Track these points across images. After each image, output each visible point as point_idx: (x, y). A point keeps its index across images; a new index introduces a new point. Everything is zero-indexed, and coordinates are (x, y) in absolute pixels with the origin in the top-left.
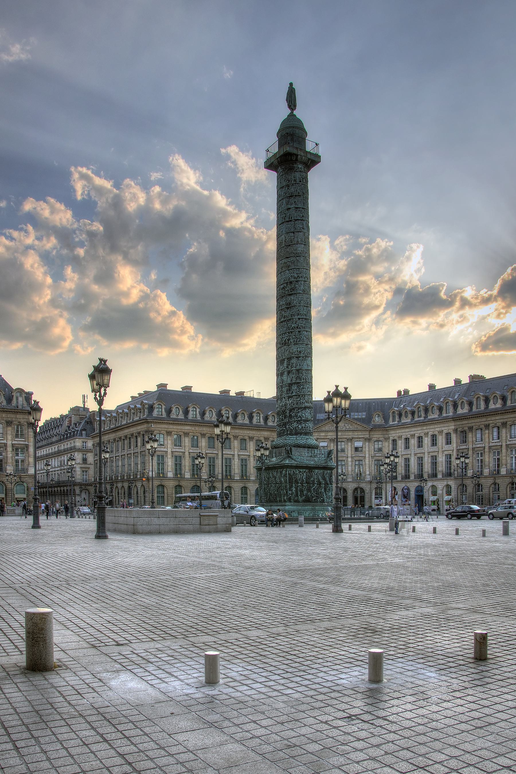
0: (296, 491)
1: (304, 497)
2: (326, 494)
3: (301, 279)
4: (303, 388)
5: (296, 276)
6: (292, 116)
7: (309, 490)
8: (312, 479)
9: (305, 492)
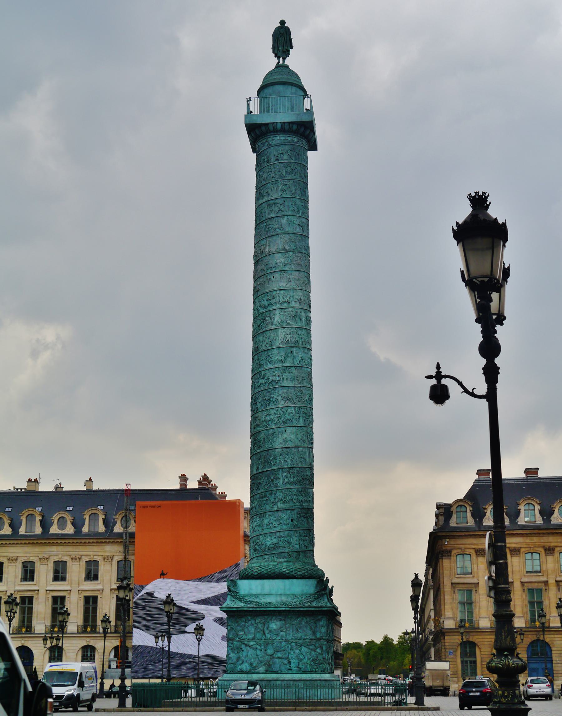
3: (274, 307)
5: (266, 303)
6: (281, 68)
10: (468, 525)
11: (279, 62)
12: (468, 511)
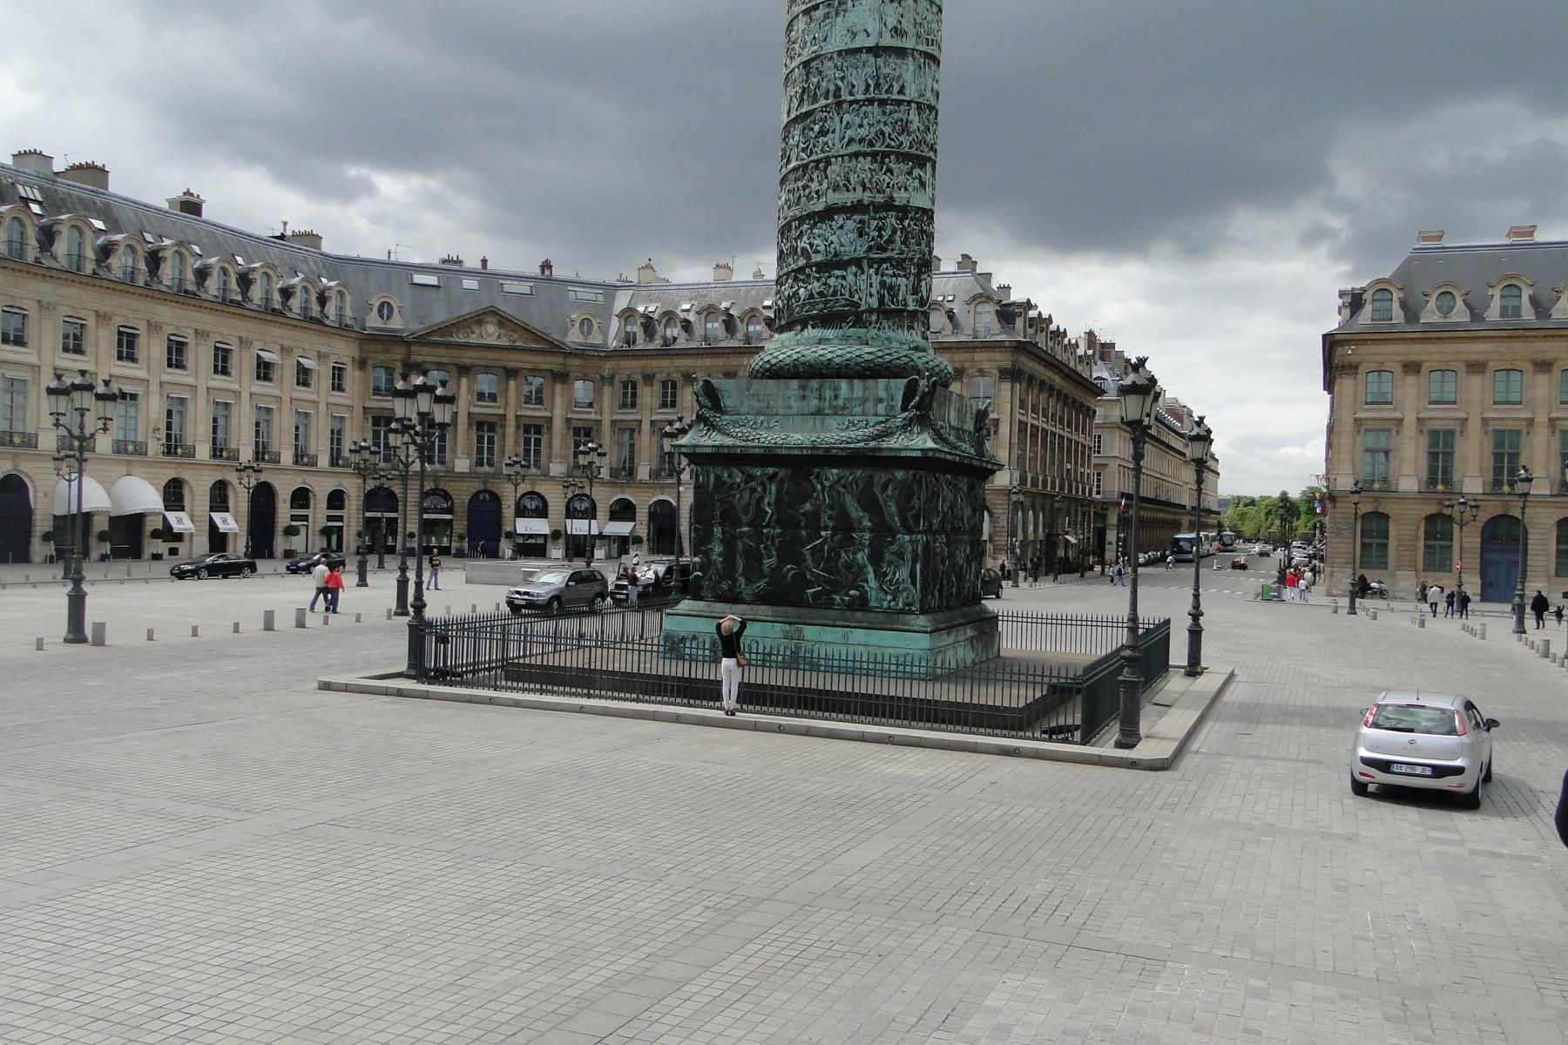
0: (729, 555)
1: (762, 583)
2: (880, 575)
4: (823, 132)
7: (790, 553)
8: (808, 507)
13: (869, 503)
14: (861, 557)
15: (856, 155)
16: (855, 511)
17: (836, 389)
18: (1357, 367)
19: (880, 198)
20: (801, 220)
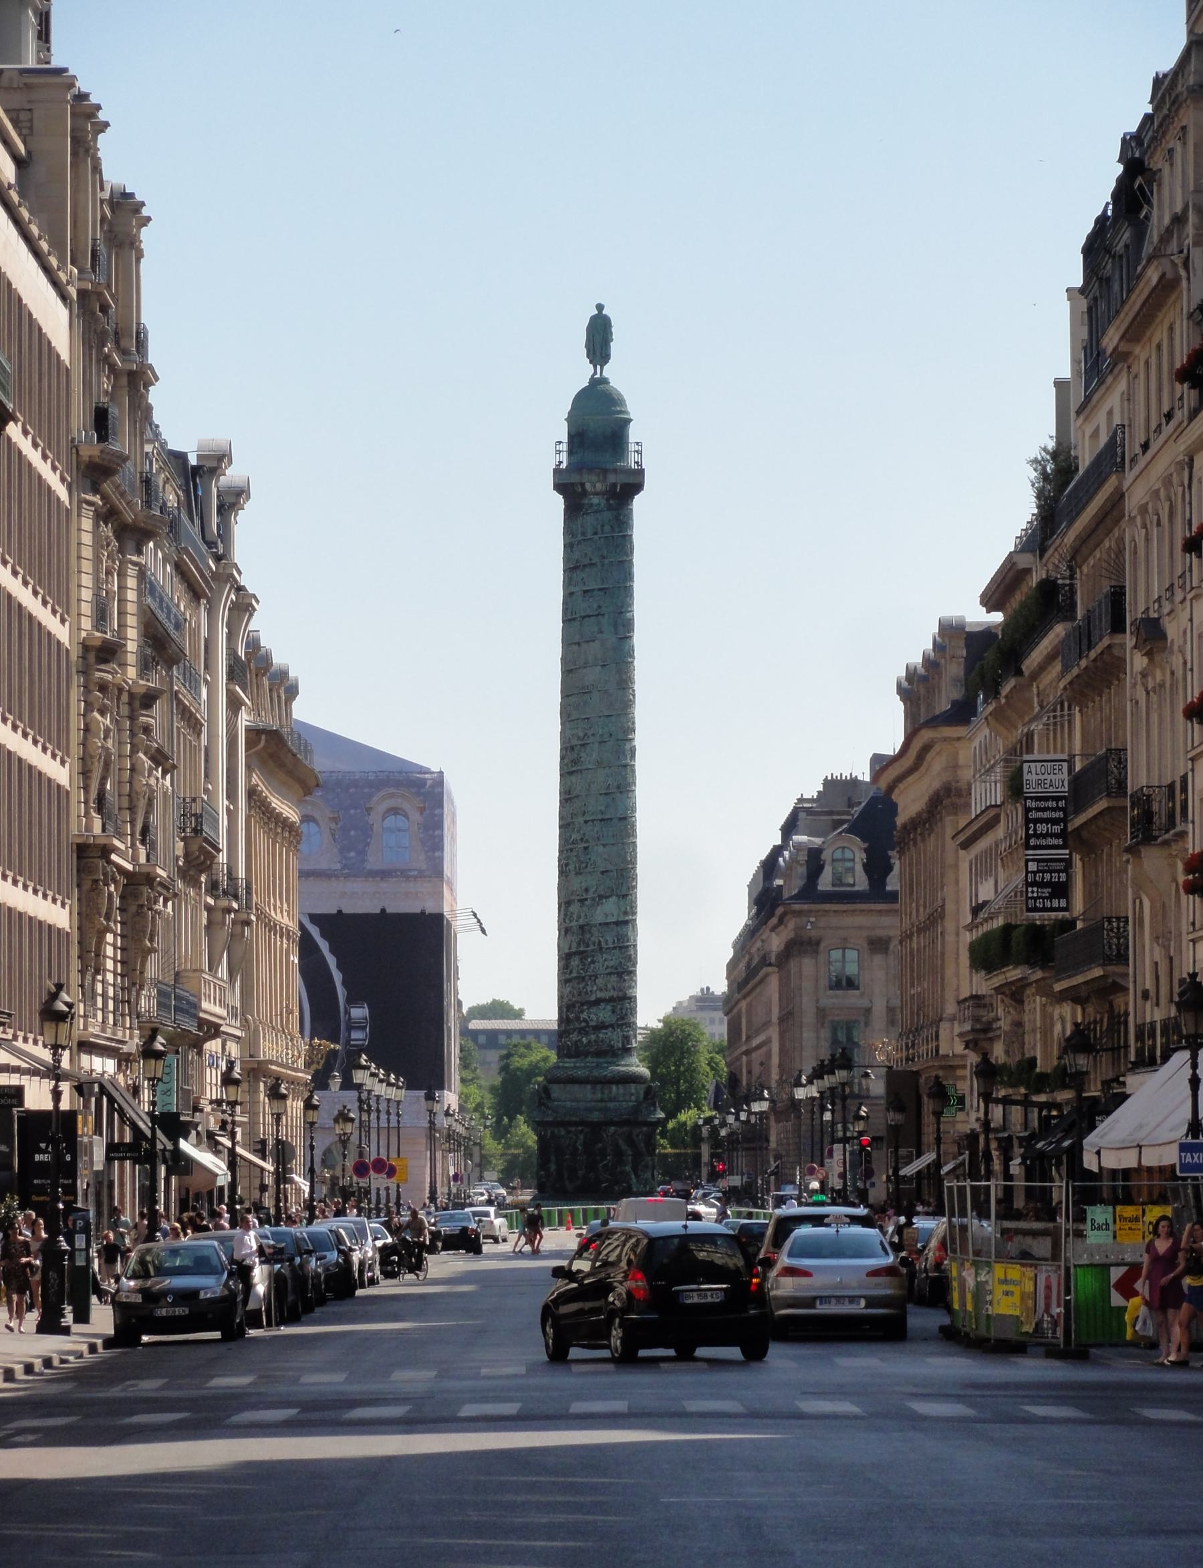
4: (593, 962)
5: (581, 734)
9: (580, 1173)
10: (856, 888)
11: (595, 373)
12: (857, 860)
13: (631, 1143)
14: (628, 1168)
15: (610, 974)
16: (624, 1147)
17: (611, 1089)
18: (818, 943)
19: (621, 994)
20: (582, 1004)
